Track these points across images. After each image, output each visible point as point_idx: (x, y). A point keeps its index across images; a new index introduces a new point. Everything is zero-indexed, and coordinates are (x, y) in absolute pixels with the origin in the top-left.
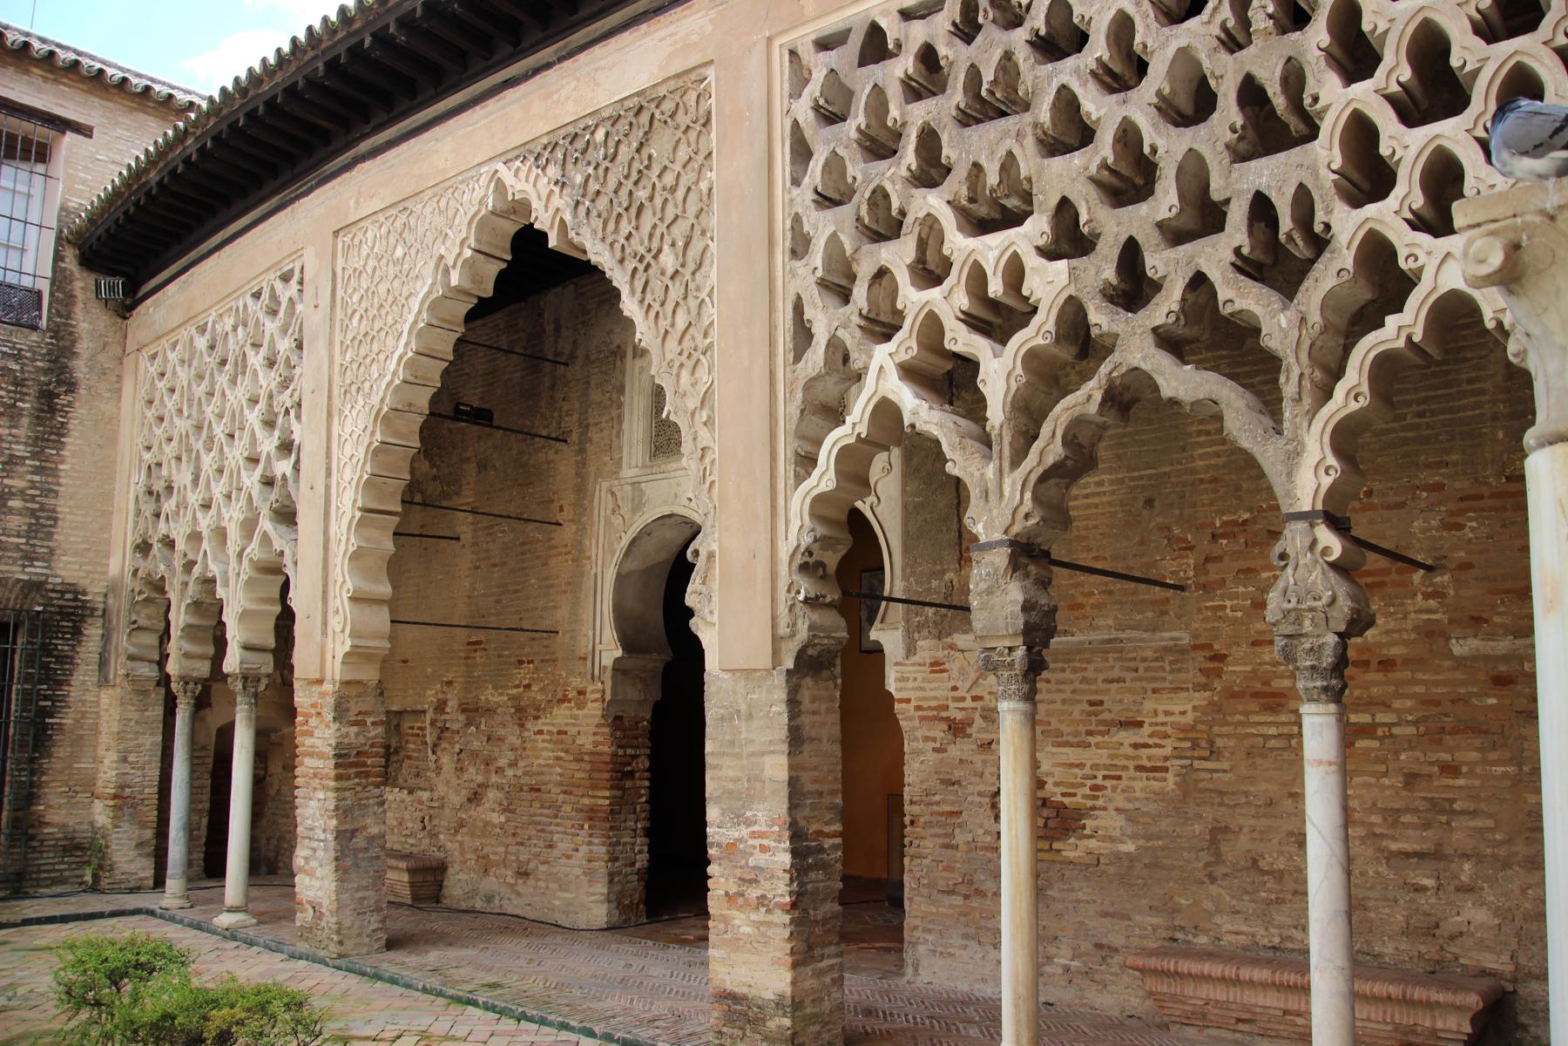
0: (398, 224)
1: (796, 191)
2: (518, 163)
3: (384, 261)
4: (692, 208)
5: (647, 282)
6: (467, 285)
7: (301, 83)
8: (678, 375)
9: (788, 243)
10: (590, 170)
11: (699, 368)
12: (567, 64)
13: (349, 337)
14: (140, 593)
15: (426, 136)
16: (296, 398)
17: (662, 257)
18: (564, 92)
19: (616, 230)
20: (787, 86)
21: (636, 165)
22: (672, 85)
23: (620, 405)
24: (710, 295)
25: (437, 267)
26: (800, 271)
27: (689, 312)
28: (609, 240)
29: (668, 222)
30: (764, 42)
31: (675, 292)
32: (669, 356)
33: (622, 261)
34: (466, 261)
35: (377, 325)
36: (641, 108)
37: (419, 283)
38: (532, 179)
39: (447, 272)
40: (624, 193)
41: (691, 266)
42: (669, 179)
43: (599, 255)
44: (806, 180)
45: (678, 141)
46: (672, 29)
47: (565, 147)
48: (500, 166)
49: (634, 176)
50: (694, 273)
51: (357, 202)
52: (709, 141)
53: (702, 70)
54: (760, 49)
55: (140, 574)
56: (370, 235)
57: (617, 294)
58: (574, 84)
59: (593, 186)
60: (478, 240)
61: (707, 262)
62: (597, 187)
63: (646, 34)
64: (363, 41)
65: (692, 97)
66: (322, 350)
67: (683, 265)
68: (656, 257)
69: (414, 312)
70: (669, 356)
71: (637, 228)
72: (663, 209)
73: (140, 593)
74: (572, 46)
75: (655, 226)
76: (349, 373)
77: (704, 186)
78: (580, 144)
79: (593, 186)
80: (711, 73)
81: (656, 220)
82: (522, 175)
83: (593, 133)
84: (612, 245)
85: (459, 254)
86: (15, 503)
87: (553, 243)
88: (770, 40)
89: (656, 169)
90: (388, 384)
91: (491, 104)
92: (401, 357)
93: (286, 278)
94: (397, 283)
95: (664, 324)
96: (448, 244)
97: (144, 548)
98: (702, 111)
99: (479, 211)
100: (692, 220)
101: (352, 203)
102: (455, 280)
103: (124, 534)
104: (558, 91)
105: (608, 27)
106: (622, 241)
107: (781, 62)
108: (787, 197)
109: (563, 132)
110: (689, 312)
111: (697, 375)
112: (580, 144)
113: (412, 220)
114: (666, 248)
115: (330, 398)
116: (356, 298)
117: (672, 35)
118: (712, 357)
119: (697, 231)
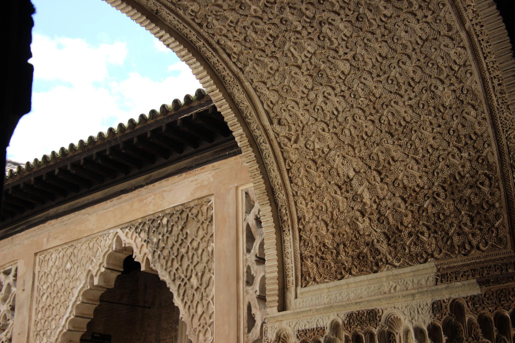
0: (68, 252)
1: (248, 256)
2: (127, 230)
3: (61, 270)
4: (205, 259)
5: (185, 291)
6: (102, 284)
7: (22, 186)
8: (198, 335)
9: (245, 278)
10: (160, 237)
11: (207, 333)
12: (150, 186)
13: (41, 306)
15: (83, 211)
16: (9, 336)
17: (192, 280)
18: (149, 200)
19: (172, 266)
20: (244, 208)
21: (181, 237)
22: (196, 202)
23: (176, 330)
24: (212, 299)
25: (87, 275)
26: (250, 291)
27: (203, 306)
28: (168, 270)
29: (194, 264)
30: (235, 189)
31: (197, 297)
32: (194, 326)
33: (174, 280)
34: (102, 273)
35: (56, 301)
36: (183, 211)
37: (78, 282)
38: (134, 238)
39: (92, 277)
40: (175, 249)
41: (204, 285)
42: (195, 244)
43: (164, 276)
44: (252, 251)
45: (199, 228)
46: (196, 177)
47: (149, 225)
48: (119, 230)
49: (180, 242)
50: (205, 289)
51: (48, 240)
52: (212, 229)
53: (209, 197)
54: (233, 191)
56: (54, 256)
57: (171, 295)
58: (153, 197)
59: (162, 245)
60: (108, 264)
61: (211, 284)
62: (163, 245)
63: (185, 178)
64: (54, 171)
65: (204, 208)
66: (26, 313)
67: (201, 285)
68: (189, 280)
69: (75, 296)
70: (194, 326)
71: (181, 265)
72: (192, 258)
74: (152, 178)
75: (189, 265)
76: (39, 325)
77: (210, 249)
78: (156, 224)
79: (162, 245)
80: (213, 199)
81: (189, 263)
82: (129, 235)
83: (161, 220)
84: (170, 272)
85: (98, 270)
87: (143, 268)
88: (237, 188)
89: (189, 239)
90: (60, 332)
91: (115, 200)
92: (67, 318)
93: (7, 273)
94: (67, 281)
95: (192, 311)
96: (93, 264)
98: (209, 215)
99: (109, 250)
100: (205, 264)
101: (45, 240)
102: (96, 282)
104: (146, 199)
105: (168, 172)
106: (174, 271)
107: (242, 198)
108: (245, 257)
109: (148, 218)
110: (203, 306)
111: (207, 336)
112: (156, 224)
113: (76, 251)
114: (193, 276)
115: (28, 337)
116: (45, 287)
117: (196, 180)
118: (213, 327)
119: (207, 270)
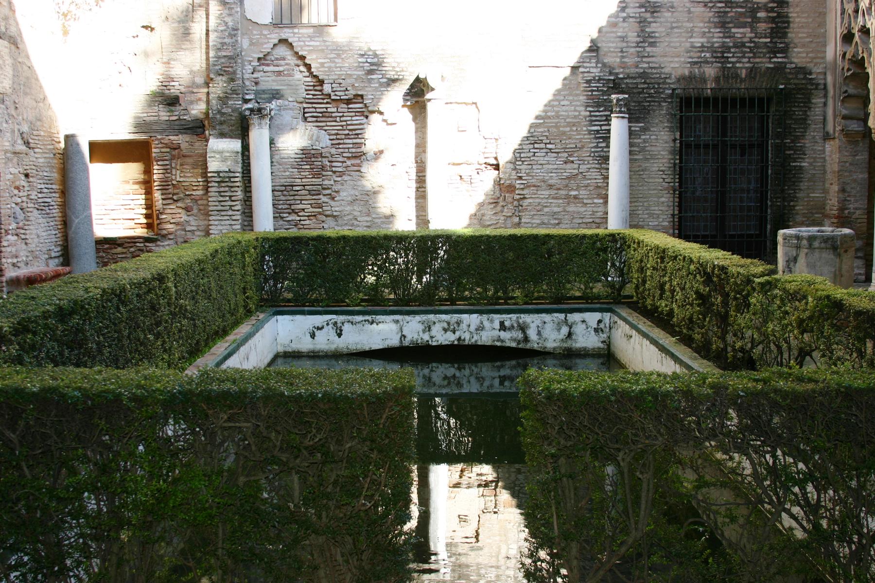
14: (848, 70)
55: (848, 56)
73: (848, 70)
86: (761, 14)
97: (848, 38)
103: (835, 28)
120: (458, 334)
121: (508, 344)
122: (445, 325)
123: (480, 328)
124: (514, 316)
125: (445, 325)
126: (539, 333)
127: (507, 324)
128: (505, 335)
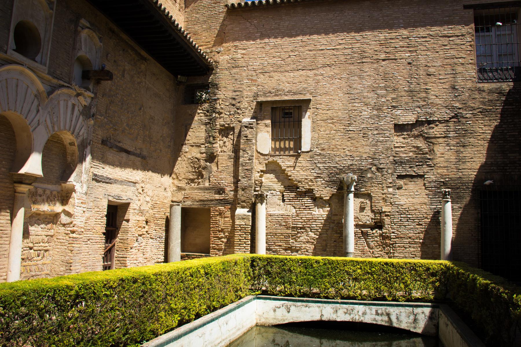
120: (352, 316)
121: (379, 323)
122: (345, 310)
123: (364, 314)
124: (383, 308)
125: (345, 310)
126: (397, 318)
127: (379, 312)
128: (379, 318)
